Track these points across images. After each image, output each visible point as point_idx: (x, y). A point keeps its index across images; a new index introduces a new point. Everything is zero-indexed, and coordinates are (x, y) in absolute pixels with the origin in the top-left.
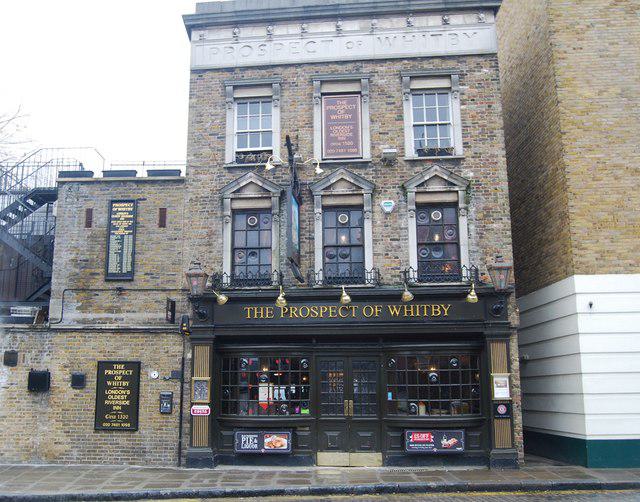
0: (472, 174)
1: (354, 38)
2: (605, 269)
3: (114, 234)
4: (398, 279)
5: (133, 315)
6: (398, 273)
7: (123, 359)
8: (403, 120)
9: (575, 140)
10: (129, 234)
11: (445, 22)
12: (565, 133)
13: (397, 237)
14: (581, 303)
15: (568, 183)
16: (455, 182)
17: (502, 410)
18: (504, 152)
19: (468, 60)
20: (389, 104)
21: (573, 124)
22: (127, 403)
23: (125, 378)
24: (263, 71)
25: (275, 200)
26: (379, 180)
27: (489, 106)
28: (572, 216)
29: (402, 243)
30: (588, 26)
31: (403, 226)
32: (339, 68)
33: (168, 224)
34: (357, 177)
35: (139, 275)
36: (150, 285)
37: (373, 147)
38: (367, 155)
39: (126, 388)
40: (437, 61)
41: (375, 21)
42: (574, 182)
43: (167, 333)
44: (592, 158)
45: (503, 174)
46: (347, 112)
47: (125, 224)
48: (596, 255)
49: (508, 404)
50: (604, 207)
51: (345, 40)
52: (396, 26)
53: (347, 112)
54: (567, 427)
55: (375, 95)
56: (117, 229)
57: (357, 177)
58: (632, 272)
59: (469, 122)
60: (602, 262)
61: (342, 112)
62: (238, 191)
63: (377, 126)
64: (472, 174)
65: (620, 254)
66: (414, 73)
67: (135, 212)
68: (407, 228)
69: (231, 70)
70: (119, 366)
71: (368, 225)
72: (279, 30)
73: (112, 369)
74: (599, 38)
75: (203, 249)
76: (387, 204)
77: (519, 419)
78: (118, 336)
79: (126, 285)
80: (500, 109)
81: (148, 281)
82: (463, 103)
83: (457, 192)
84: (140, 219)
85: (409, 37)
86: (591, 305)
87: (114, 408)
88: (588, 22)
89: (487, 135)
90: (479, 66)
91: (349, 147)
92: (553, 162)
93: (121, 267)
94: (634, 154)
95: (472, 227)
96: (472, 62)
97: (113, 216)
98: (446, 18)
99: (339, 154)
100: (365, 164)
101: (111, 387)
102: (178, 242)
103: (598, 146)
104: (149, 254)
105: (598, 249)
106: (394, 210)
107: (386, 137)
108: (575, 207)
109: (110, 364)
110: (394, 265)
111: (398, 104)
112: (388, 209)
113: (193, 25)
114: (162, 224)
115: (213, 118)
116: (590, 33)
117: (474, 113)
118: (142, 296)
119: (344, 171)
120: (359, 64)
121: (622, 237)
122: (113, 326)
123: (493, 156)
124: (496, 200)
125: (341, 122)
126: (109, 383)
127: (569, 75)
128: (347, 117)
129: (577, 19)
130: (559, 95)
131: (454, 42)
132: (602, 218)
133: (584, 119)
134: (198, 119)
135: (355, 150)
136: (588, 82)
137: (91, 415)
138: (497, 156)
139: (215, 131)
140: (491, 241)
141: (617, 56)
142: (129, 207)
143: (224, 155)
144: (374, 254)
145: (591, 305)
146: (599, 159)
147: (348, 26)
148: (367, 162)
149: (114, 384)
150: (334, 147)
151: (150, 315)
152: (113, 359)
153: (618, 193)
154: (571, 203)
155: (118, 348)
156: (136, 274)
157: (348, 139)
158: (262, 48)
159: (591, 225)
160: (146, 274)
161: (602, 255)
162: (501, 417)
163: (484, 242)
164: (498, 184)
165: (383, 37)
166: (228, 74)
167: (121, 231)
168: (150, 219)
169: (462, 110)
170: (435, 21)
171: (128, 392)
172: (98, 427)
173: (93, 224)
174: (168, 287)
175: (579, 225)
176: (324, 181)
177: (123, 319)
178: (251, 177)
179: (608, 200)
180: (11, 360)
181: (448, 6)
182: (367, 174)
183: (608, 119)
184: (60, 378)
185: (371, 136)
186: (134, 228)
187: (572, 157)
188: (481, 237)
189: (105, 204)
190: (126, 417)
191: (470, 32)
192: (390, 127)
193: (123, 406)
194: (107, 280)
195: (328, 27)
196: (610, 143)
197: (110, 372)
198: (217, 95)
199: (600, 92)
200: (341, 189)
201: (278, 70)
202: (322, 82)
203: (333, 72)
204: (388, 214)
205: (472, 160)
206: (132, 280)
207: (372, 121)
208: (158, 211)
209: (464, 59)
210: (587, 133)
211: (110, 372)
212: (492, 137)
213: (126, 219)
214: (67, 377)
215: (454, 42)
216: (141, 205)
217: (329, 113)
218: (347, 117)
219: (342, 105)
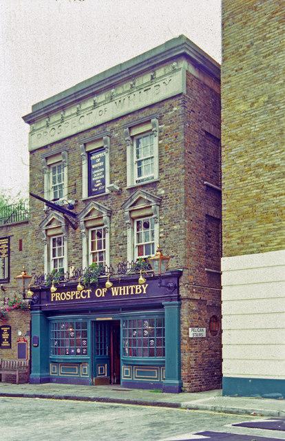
0: (163, 192)
2: (243, 251)
9: (231, 150)
20: (119, 150)
30: (248, 47)
32: (95, 131)
33: (23, 249)
44: (241, 163)
48: (239, 241)
50: (246, 201)
51: (100, 109)
59: (163, 153)
60: (242, 246)
64: (163, 192)
66: (130, 125)
67: (9, 244)
75: (36, 261)
82: (160, 140)
84: (11, 248)
85: (132, 96)
94: (272, 153)
96: (167, 104)
102: (27, 258)
103: (246, 152)
113: (29, 119)
114: (21, 249)
116: (251, 52)
120: (105, 125)
129: (240, 43)
142: (6, 241)
144: (111, 256)
148: (107, 195)
168: (14, 246)
169: (159, 144)
170: (146, 78)
182: (108, 203)
188: (167, 237)
192: (119, 171)
199: (253, 104)
200: (94, 216)
202: (85, 144)
207: (111, 165)
216: (12, 239)
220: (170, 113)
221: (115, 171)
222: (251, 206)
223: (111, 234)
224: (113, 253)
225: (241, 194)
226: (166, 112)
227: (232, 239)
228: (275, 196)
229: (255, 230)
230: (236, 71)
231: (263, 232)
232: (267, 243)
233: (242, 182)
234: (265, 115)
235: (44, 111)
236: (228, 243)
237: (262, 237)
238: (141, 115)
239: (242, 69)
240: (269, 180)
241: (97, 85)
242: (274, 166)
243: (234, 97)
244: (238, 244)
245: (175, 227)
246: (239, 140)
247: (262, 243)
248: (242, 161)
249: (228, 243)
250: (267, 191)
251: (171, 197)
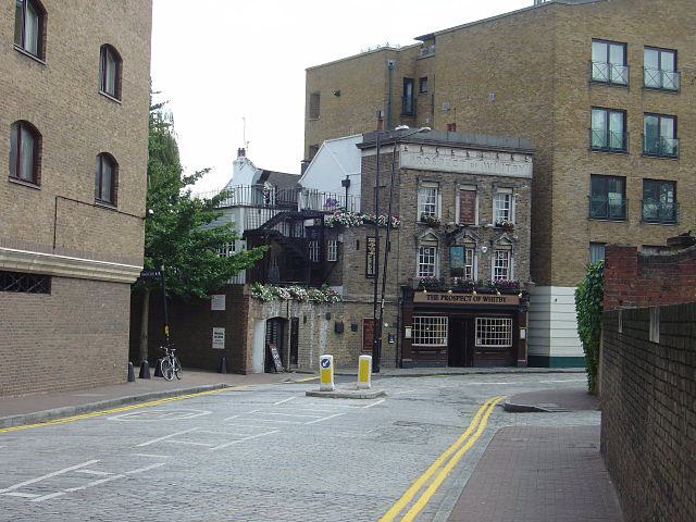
54: (541, 352)
69: (420, 171)
108: (554, 256)
125: (466, 205)
161: (562, 278)
180: (328, 317)
184: (347, 326)
195: (463, 153)
217: (461, 200)
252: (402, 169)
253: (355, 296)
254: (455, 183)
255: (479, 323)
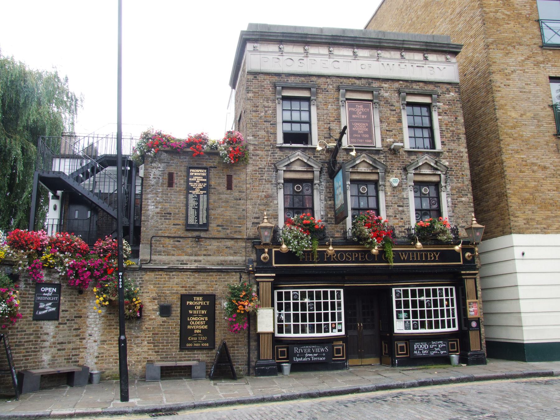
1: (366, 62)
2: (530, 231)
3: (191, 193)
4: (403, 234)
5: (209, 258)
6: (403, 230)
7: (201, 292)
8: (401, 122)
9: (508, 145)
10: (204, 194)
11: (426, 59)
12: (502, 140)
13: (401, 204)
14: (517, 253)
15: (505, 173)
16: (439, 168)
17: (474, 324)
18: (466, 150)
19: (441, 85)
21: (507, 134)
22: (206, 327)
23: (203, 308)
24: (303, 79)
25: (317, 173)
26: (388, 164)
27: (456, 118)
28: (509, 195)
29: (405, 209)
30: (512, 72)
31: (405, 197)
32: (357, 82)
34: (374, 161)
35: (213, 226)
36: (221, 235)
37: (382, 140)
38: (379, 145)
39: (204, 315)
40: (421, 84)
41: (379, 52)
42: (509, 173)
43: (236, 272)
44: (519, 158)
45: (466, 165)
46: (363, 113)
47: (201, 186)
49: (478, 320)
51: (360, 62)
52: (393, 57)
53: (363, 113)
55: (382, 103)
56: (194, 189)
57: (374, 161)
58: (546, 233)
60: (527, 226)
61: (360, 113)
62: (288, 165)
63: (385, 125)
65: (538, 221)
66: (407, 91)
68: (408, 198)
69: (278, 75)
70: (198, 298)
71: (382, 195)
72: (313, 50)
73: (192, 300)
74: (519, 80)
75: (262, 207)
76: (394, 181)
77: (483, 330)
78: (196, 275)
79: (203, 234)
80: (463, 121)
81: (219, 231)
83: (440, 175)
84: (212, 183)
85: (402, 65)
86: (523, 254)
87: (195, 331)
88: (513, 68)
89: (455, 137)
90: (448, 91)
91: (366, 138)
92: (491, 159)
93: (198, 219)
95: (449, 200)
97: (190, 179)
98: (426, 55)
99: (359, 143)
100: (378, 152)
101: (192, 315)
102: (242, 202)
103: (522, 150)
104: (219, 211)
105: (525, 217)
106: (399, 185)
107: (391, 133)
108: (511, 189)
109: (190, 297)
110: (401, 224)
111: (398, 111)
112: (396, 184)
115: (267, 109)
116: (513, 76)
117: (446, 122)
118: (215, 244)
119: (365, 155)
120: (370, 81)
121: (539, 209)
122: (193, 266)
123: (459, 152)
124: (463, 182)
125: (360, 120)
126: (191, 312)
127: (502, 102)
128: (363, 117)
130: (497, 115)
131: (432, 72)
132: (527, 197)
133: (513, 131)
134: (254, 109)
135: (370, 141)
136: (514, 108)
137: (177, 337)
138: (462, 152)
139: (269, 119)
140: (460, 208)
141: (530, 92)
142: (203, 173)
143: (275, 137)
145: (523, 254)
146: (523, 158)
147: (362, 53)
149: (195, 312)
150: (356, 138)
151: (222, 258)
152: (193, 292)
153: (535, 181)
154: (507, 187)
155: (196, 284)
156: (211, 225)
157: (365, 132)
158: (301, 61)
159: (520, 201)
160: (218, 226)
161: (528, 221)
162: (474, 329)
163: (457, 210)
164: (464, 171)
165: (385, 64)
166: (275, 79)
167: (197, 192)
169: (439, 119)
170: (419, 56)
171: (206, 319)
172: (182, 348)
173: (175, 185)
174: (236, 236)
175: (514, 201)
176: (352, 161)
177: (200, 261)
178: (298, 155)
179: (529, 185)
181: (428, 48)
182: (380, 158)
183: (527, 132)
185: (381, 131)
186: (207, 189)
187: (507, 156)
189: (183, 169)
190: (205, 338)
191: (441, 67)
193: (202, 329)
194: (187, 230)
195: (348, 52)
196: (529, 149)
197: (191, 303)
198: (268, 92)
199: (521, 115)
201: (314, 79)
203: (352, 84)
204: (395, 187)
205: (447, 154)
206: (207, 230)
207: (381, 121)
208: (226, 177)
209: (439, 85)
210: (515, 141)
211: (191, 303)
212: (459, 139)
213: (201, 182)
214: (156, 307)
215: (432, 72)
217: (351, 113)
218: (363, 117)
219: (360, 108)
220: (447, 96)
221: (387, 128)
222: (531, 194)
223: (386, 193)
224: (390, 214)
225: (522, 183)
226: (443, 93)
227: (519, 219)
228: (549, 190)
229: (537, 214)
230: (505, 85)
231: (544, 217)
232: (548, 227)
233: (521, 174)
234: (533, 127)
235: (283, 36)
236: (515, 221)
237: (544, 222)
238: (415, 86)
239: (509, 86)
240: (543, 177)
241: (412, 43)
242: (545, 168)
243: (506, 105)
244: (525, 224)
245: (463, 199)
246: (514, 139)
247: (545, 226)
248: (519, 156)
249: (515, 221)
250: (544, 186)
251: (457, 171)
252: (250, 73)
253: (164, 258)
254: (338, 89)
255: (398, 295)
